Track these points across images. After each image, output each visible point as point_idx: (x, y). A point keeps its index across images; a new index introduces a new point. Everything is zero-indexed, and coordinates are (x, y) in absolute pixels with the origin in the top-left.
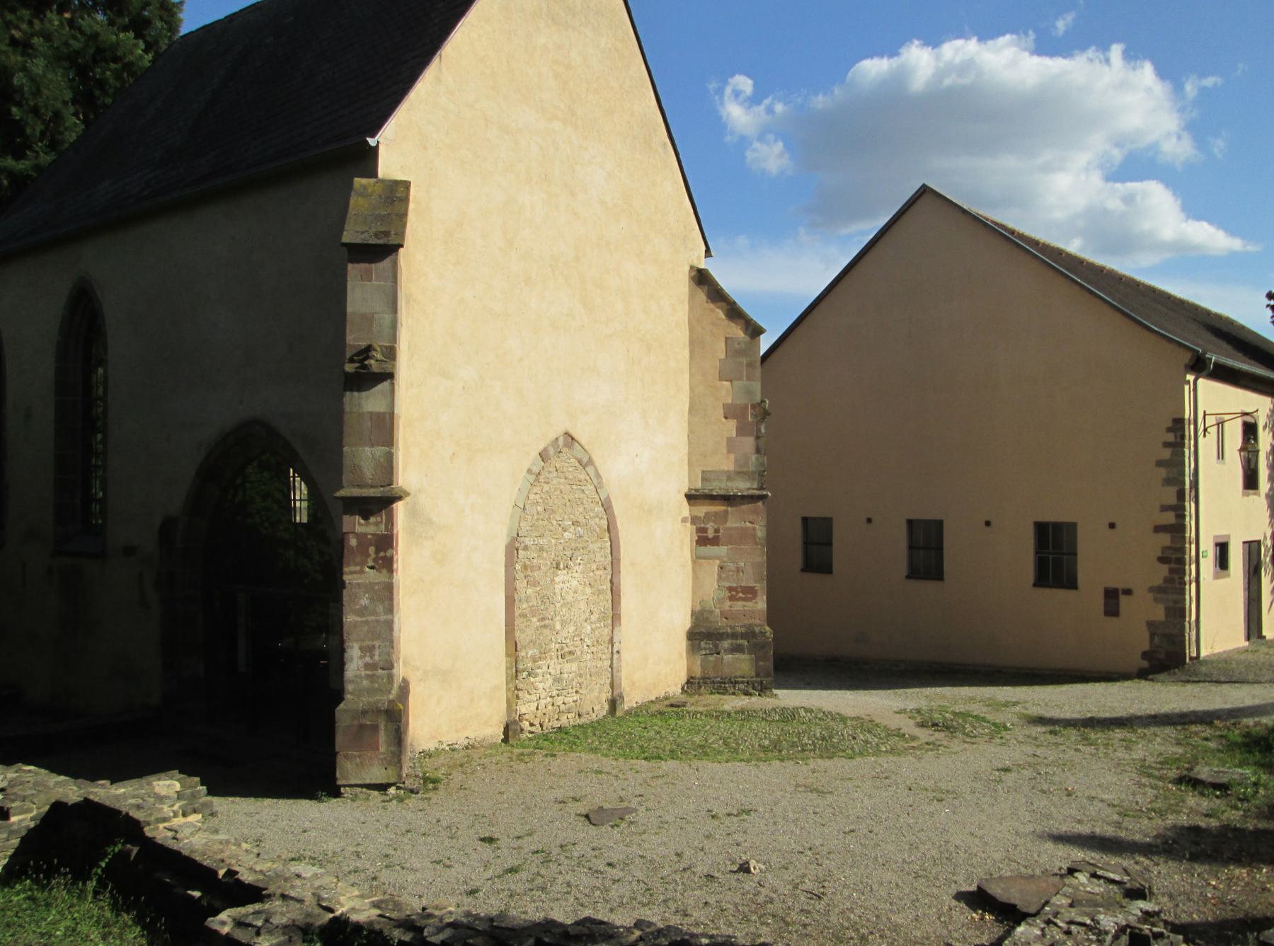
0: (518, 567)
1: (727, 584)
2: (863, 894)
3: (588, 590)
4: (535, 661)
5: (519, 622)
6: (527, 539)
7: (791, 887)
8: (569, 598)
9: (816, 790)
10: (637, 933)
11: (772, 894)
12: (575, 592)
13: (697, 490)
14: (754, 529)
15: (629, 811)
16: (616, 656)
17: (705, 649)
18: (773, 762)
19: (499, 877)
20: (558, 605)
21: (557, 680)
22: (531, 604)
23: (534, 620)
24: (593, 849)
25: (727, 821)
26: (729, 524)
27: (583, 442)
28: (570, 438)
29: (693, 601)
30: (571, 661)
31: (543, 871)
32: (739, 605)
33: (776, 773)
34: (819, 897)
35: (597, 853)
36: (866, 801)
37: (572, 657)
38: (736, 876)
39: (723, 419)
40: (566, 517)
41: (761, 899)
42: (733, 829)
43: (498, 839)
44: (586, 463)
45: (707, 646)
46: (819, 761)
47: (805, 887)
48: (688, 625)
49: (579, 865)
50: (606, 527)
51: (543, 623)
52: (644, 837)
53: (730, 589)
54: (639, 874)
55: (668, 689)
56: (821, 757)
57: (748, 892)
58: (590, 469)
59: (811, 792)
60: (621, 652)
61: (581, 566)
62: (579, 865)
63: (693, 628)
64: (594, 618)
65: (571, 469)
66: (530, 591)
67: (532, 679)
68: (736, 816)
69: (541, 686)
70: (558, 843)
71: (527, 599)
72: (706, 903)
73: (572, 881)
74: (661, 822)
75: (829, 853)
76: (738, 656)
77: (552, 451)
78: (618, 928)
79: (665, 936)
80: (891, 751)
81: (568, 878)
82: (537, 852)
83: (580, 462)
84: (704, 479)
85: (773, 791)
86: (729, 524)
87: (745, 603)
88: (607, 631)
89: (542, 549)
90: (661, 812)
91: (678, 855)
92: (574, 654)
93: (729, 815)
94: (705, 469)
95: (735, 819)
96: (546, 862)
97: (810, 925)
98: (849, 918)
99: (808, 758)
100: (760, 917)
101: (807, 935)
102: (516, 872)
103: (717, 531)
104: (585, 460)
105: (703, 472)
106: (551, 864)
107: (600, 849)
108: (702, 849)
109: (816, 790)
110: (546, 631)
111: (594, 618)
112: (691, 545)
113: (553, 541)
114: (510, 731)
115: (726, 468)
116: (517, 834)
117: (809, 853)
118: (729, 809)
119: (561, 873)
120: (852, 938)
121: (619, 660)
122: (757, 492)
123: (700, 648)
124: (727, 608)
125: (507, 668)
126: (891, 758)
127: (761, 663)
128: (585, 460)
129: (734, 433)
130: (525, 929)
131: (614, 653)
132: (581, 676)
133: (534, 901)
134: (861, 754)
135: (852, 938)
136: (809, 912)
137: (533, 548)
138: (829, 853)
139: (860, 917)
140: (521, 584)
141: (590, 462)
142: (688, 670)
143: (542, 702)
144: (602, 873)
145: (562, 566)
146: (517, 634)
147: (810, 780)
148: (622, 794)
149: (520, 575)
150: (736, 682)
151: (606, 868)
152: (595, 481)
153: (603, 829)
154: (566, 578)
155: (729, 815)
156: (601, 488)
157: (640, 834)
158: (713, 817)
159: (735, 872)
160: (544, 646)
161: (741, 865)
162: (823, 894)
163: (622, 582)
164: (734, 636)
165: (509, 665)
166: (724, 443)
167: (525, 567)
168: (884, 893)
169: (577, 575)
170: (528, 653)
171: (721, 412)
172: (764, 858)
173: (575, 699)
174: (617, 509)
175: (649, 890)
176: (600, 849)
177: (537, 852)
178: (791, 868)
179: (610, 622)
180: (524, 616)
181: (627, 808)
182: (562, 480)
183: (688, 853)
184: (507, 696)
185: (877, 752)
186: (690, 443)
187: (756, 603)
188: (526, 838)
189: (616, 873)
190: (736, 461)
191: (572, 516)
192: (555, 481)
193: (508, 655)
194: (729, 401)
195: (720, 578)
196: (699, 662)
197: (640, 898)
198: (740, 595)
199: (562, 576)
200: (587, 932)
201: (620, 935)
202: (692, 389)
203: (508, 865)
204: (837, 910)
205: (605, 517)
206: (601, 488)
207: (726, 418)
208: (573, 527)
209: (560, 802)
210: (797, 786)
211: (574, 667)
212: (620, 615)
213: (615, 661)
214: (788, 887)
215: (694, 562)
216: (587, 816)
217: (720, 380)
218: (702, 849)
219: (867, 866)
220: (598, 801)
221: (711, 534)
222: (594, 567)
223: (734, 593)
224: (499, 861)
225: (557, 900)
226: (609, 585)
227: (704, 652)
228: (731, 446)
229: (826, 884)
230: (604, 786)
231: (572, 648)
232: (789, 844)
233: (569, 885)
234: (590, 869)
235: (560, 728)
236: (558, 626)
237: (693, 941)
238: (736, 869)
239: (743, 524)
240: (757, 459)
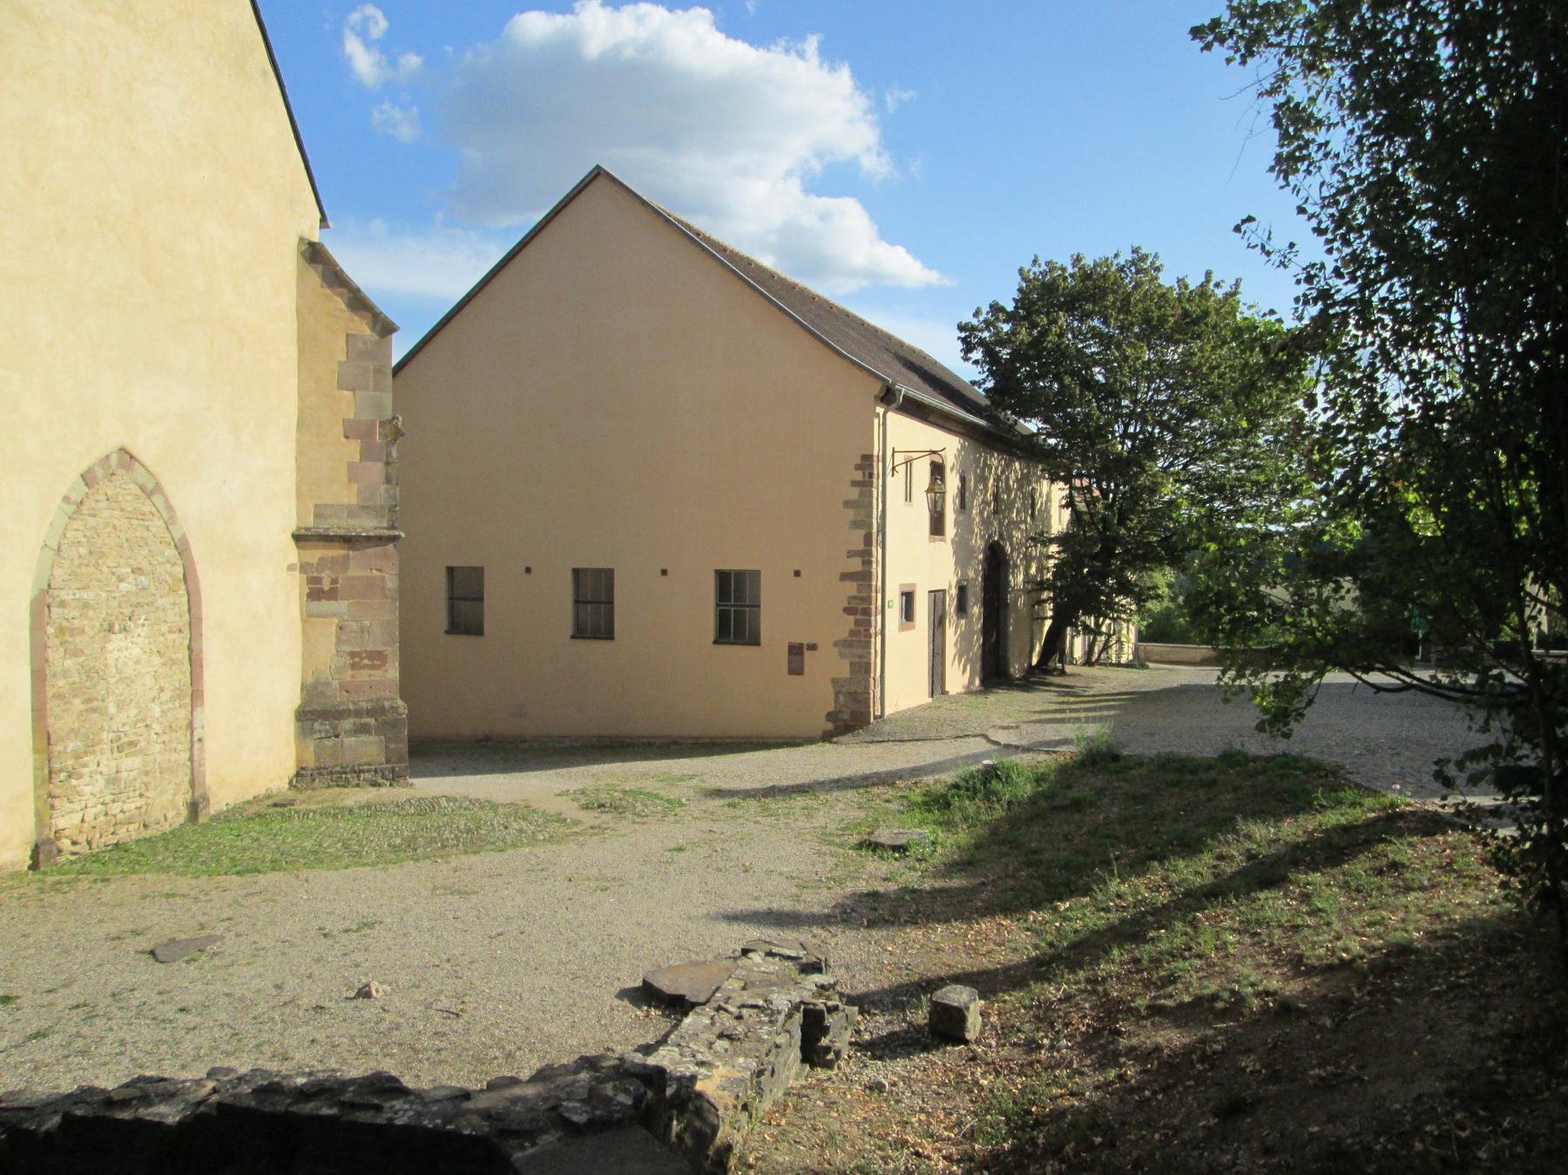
0: (50, 630)
1: (349, 649)
2: (511, 1005)
3: (156, 660)
4: (77, 757)
5: (53, 706)
6: (64, 592)
7: (422, 1008)
8: (129, 671)
9: (459, 892)
10: (211, 1085)
11: (398, 1020)
13: (307, 529)
14: (383, 579)
15: (212, 939)
16: (197, 746)
17: (320, 731)
18: (405, 864)
19: (16, 1047)
20: (112, 681)
21: (113, 781)
22: (71, 680)
23: (77, 701)
24: (160, 993)
25: (344, 939)
26: (351, 573)
27: (147, 461)
28: (127, 457)
29: (304, 671)
31: (85, 1030)
32: (364, 675)
33: (410, 876)
34: (457, 1015)
35: (165, 997)
36: (518, 899)
38: (353, 1003)
39: (343, 439)
40: (122, 562)
41: (384, 1027)
42: (351, 947)
43: (18, 997)
44: (152, 490)
45: (322, 728)
46: (463, 857)
47: (440, 1006)
48: (296, 701)
49: (137, 1016)
50: (181, 576)
51: (89, 706)
52: (231, 970)
53: (352, 655)
54: (223, 1017)
55: (270, 786)
56: (466, 852)
57: (368, 1021)
58: (158, 500)
59: (452, 893)
61: (145, 628)
62: (137, 1016)
63: (303, 704)
64: (165, 697)
65: (129, 498)
66: (69, 663)
67: (74, 782)
68: (356, 931)
69: (87, 790)
70: (109, 992)
71: (66, 674)
72: (313, 1041)
73: (128, 1038)
74: (256, 949)
75: (471, 963)
76: (363, 738)
77: (100, 473)
78: (184, 1082)
79: (247, 1082)
80: (551, 840)
81: (122, 1034)
82: (78, 1006)
83: (142, 488)
84: (317, 515)
85: (404, 898)
86: (351, 573)
87: (372, 672)
88: (183, 714)
89: (86, 606)
90: (256, 937)
91: (277, 987)
92: (136, 745)
93: (346, 931)
94: (318, 502)
95: (354, 936)
96: (90, 1018)
97: (446, 1049)
98: (493, 1035)
99: (449, 855)
100: (382, 1049)
101: (441, 1062)
102: (45, 1036)
103: (334, 581)
104: (150, 486)
105: (316, 506)
106: (97, 1021)
107: (169, 992)
108: (310, 977)
109: (459, 892)
110: (95, 717)
111: (165, 697)
112: (301, 602)
113: (104, 595)
114: (39, 855)
115: (346, 501)
116: (48, 987)
117: (447, 966)
118: (347, 925)
119: (111, 1029)
120: (496, 1058)
121: (202, 751)
122: (386, 533)
123: (312, 731)
124: (349, 679)
125: (36, 769)
126: (549, 846)
127: (392, 746)
128: (150, 486)
129: (357, 457)
130: (49, 1104)
131: (195, 742)
132: (147, 773)
133: (70, 1071)
134: (514, 845)
135: (496, 1058)
136: (444, 1034)
137: (74, 604)
138: (471, 963)
139: (506, 1032)
140: (55, 654)
141: (158, 489)
142: (299, 759)
143: (90, 813)
144: (171, 1022)
145: (117, 628)
146: (51, 721)
147: (451, 880)
148: (204, 919)
149: (53, 642)
150: (361, 771)
151: (179, 1015)
152: (165, 514)
153: (175, 966)
154: (124, 644)
155: (346, 931)
156: (174, 523)
157: (227, 967)
158: (325, 935)
159: (351, 999)
161: (360, 990)
162: (462, 1010)
163: (204, 648)
164: (358, 713)
166: (345, 469)
167: (61, 631)
168: (535, 1001)
171: (339, 430)
172: (390, 978)
173: (139, 804)
174: (197, 551)
175: (236, 1034)
176: (169, 992)
177: (78, 1006)
178: (424, 985)
179: (188, 701)
180: (60, 696)
181: (209, 936)
182: (117, 513)
183: (291, 983)
184: (36, 807)
185: (534, 841)
186: (299, 469)
187: (386, 671)
188: (61, 990)
189: (192, 1019)
190: (359, 493)
191: (132, 562)
192: (105, 514)
193: (36, 751)
194: (352, 416)
195: (339, 641)
196: (312, 748)
197: (224, 1046)
198: (366, 661)
199: (117, 641)
200: (137, 1093)
201: (187, 1091)
202: (301, 398)
203: (30, 1030)
204: (479, 1028)
205: (180, 562)
207: (346, 437)
209: (114, 939)
210: (435, 888)
211: (136, 762)
213: (196, 752)
214: (419, 1008)
215: (304, 621)
216: (152, 953)
217: (339, 388)
218: (310, 977)
219: (516, 973)
220: (168, 933)
221: (326, 586)
222: (164, 628)
223: (357, 660)
224: (19, 1026)
225: (105, 1064)
226: (186, 652)
227: (318, 735)
228: (353, 473)
229: (466, 999)
230: (178, 912)
231: (133, 738)
232: (422, 957)
233: (123, 1043)
234: (154, 1019)
235: (117, 845)
236: (112, 709)
237: (285, 1083)
238: (352, 994)
239: (368, 573)
240: (387, 491)
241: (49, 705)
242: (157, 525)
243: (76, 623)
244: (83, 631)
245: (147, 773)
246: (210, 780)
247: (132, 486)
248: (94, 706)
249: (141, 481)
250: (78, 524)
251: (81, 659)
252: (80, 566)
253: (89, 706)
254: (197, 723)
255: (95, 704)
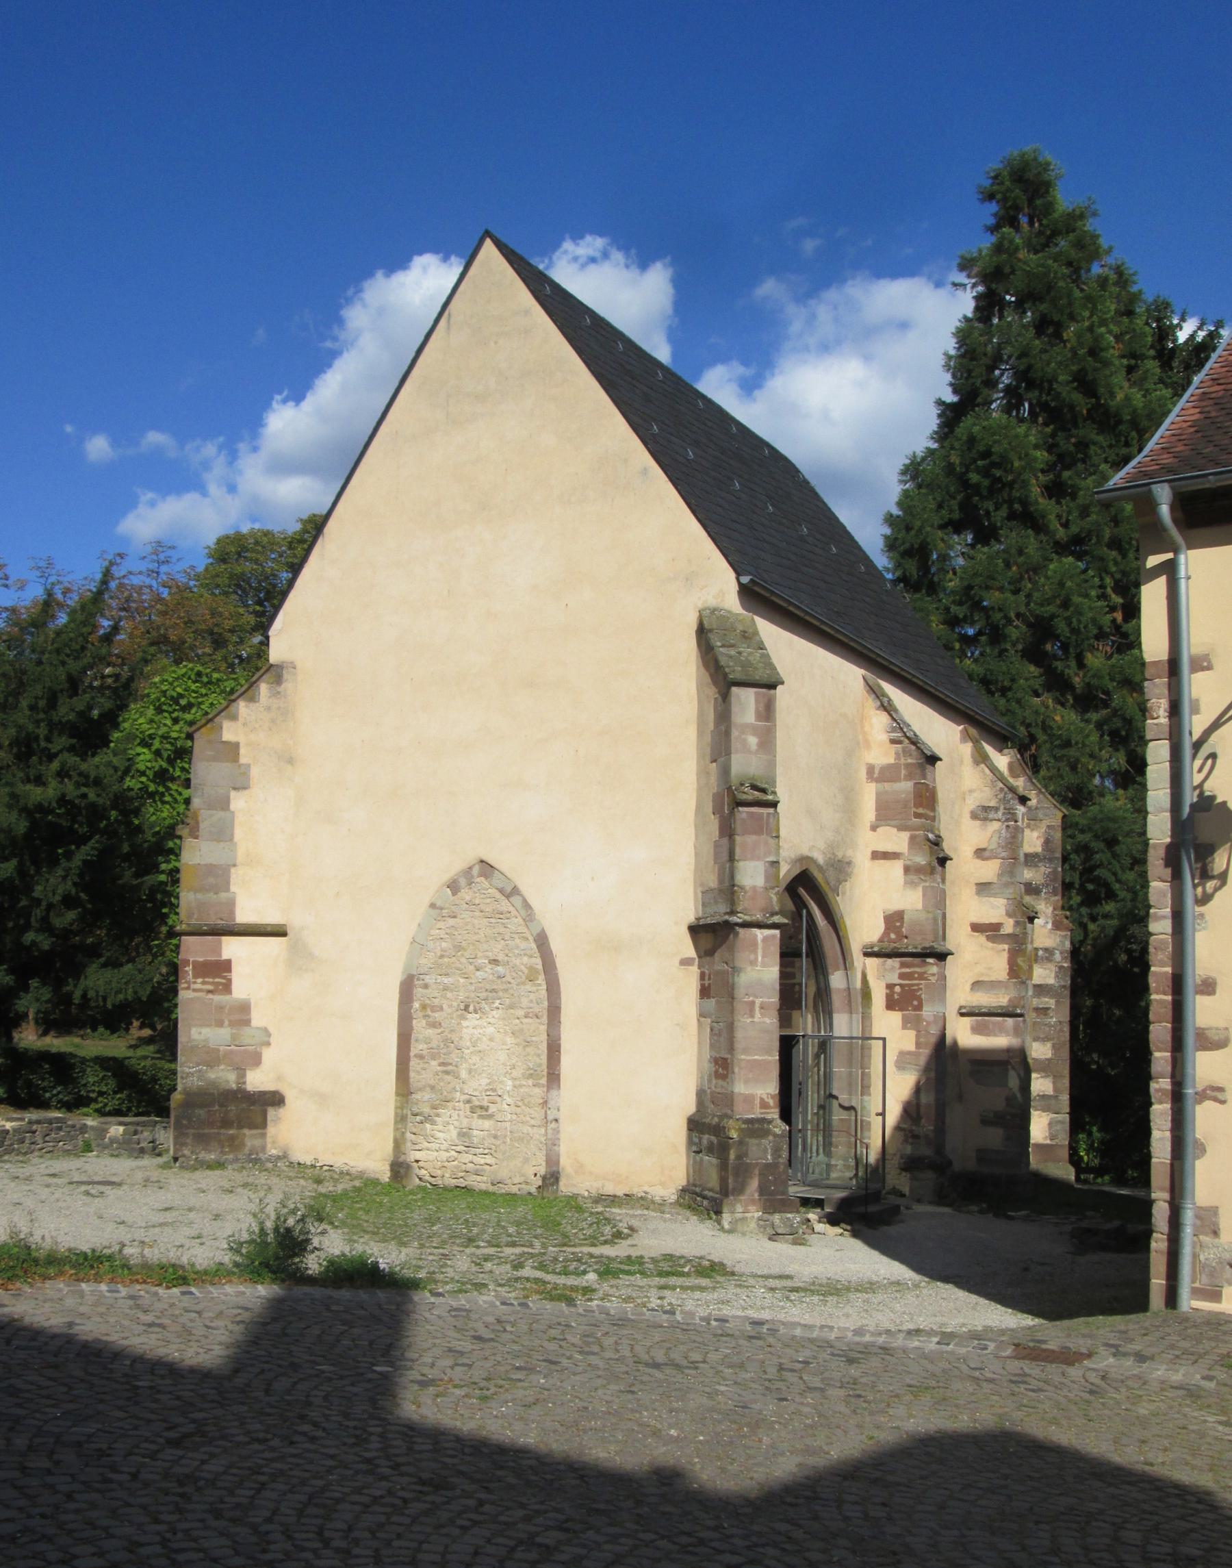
0: (416, 1005)
3: (510, 1040)
4: (434, 1107)
5: (414, 1063)
8: (481, 1046)
12: (491, 1040)
20: (466, 1051)
21: (462, 1135)
22: (430, 1045)
23: (434, 1063)
28: (486, 867)
30: (480, 1117)
37: (484, 1113)
40: (480, 954)
44: (512, 892)
48: (691, 1108)
50: (540, 967)
51: (445, 1068)
58: (516, 900)
60: (560, 1121)
63: (693, 1115)
64: (517, 1073)
65: (488, 901)
66: (430, 1032)
67: (428, 1126)
71: (427, 1041)
77: (463, 882)
83: (501, 891)
110: (448, 1078)
111: (515, 1073)
113: (462, 980)
125: (396, 1108)
128: (509, 889)
131: (551, 1122)
132: (495, 1137)
140: (419, 1025)
141: (515, 891)
145: (471, 1009)
146: (412, 1074)
152: (523, 913)
160: (445, 1093)
165: (399, 1104)
167: (424, 1007)
169: (492, 1020)
170: (423, 1099)
174: (555, 945)
179: (544, 1081)
180: (421, 1057)
182: (477, 913)
192: (466, 915)
193: (397, 1094)
199: (472, 1020)
205: (538, 954)
206: (531, 921)
208: (490, 966)
211: (487, 1124)
212: (559, 1075)
222: (521, 1013)
231: (485, 1104)
236: (464, 1074)
241: (412, 1063)
242: (516, 923)
243: (436, 1002)
244: (442, 1009)
245: (495, 1137)
246: (565, 1163)
247: (492, 891)
248: (448, 1069)
249: (500, 886)
250: (441, 924)
251: (440, 1031)
252: (442, 957)
253: (445, 1068)
254: (551, 1104)
255: (450, 1068)
